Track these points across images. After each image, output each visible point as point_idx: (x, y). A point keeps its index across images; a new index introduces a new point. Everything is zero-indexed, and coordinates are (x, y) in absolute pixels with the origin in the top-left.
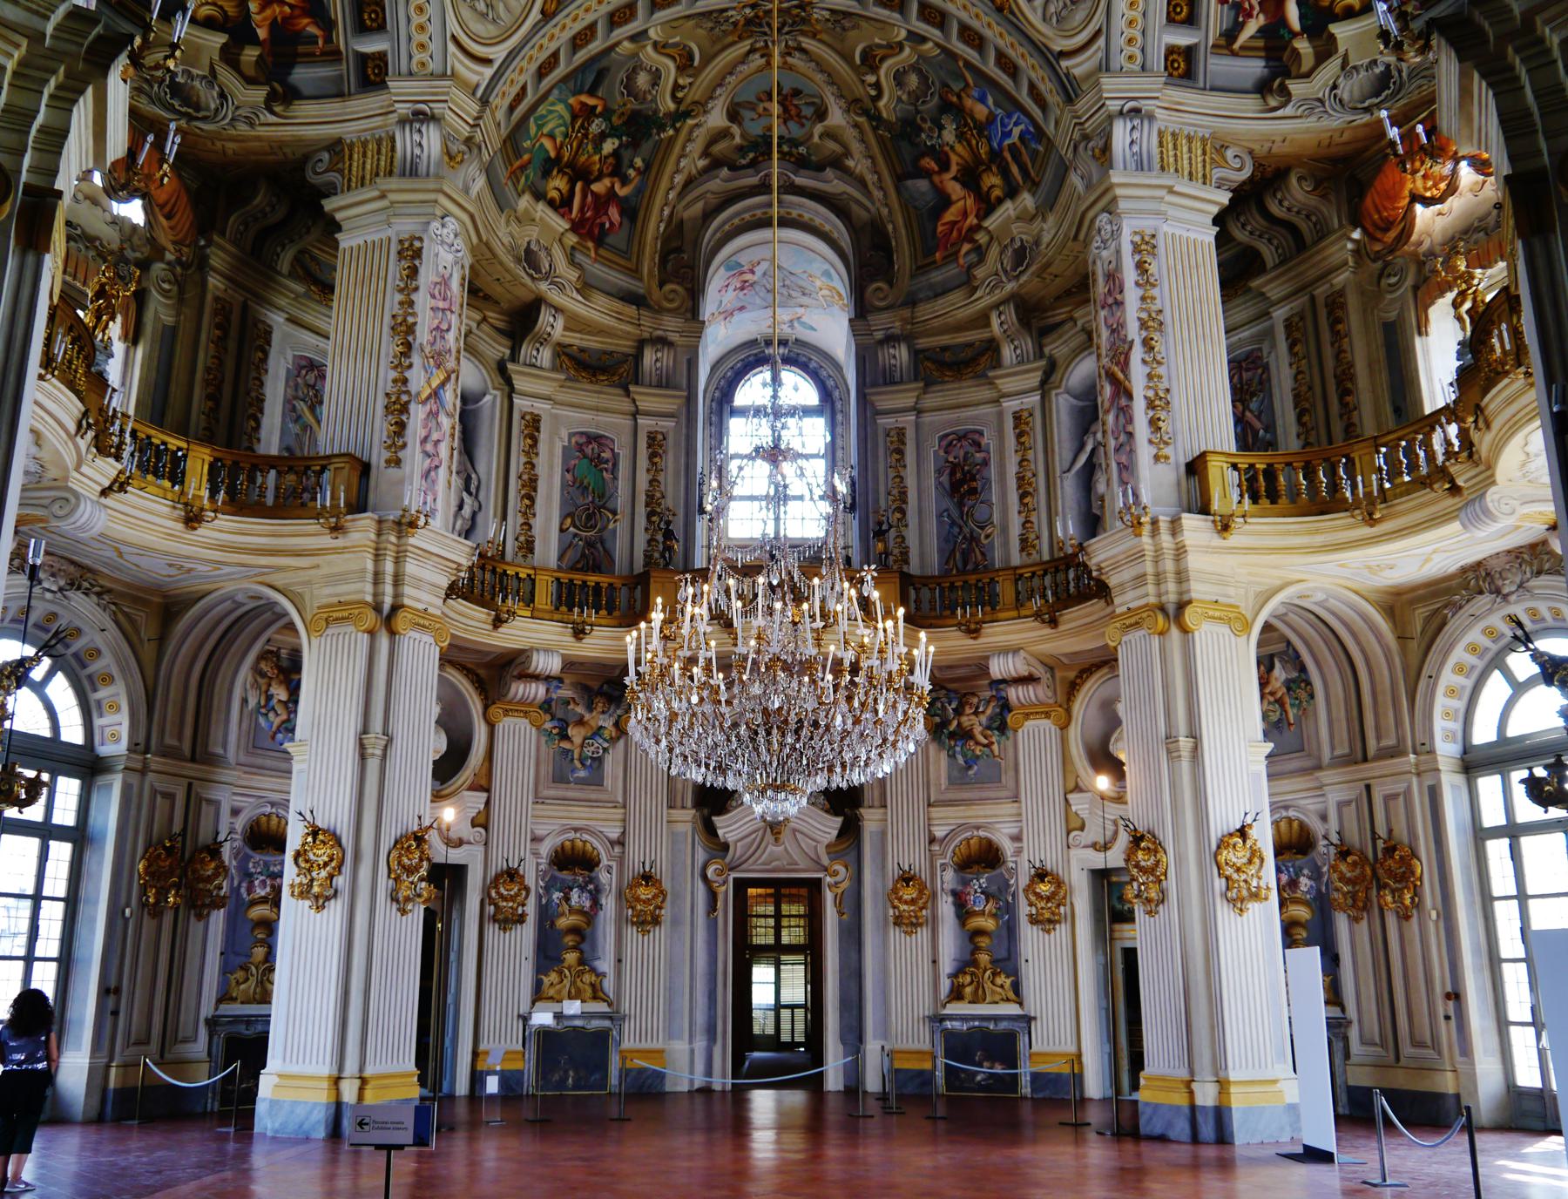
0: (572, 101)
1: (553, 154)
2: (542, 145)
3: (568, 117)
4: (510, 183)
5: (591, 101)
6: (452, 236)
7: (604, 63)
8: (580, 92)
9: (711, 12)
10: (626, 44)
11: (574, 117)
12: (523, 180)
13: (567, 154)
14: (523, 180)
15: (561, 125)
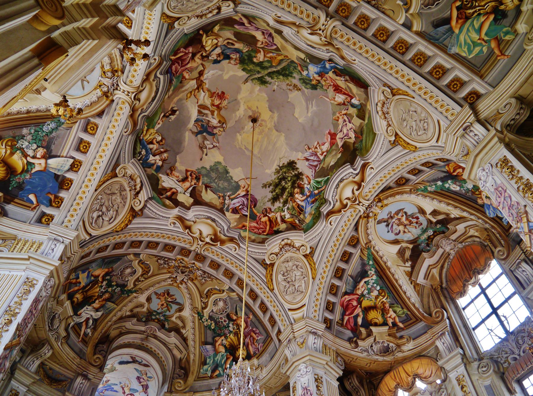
0: (457, 31)
1: (492, 17)
2: (486, 34)
3: (470, 21)
4: (507, 54)
5: (455, 13)
6: (484, 173)
7: (431, 30)
8: (451, 30)
9: (373, 6)
10: (415, 28)
11: (467, 18)
12: (507, 38)
13: (491, 4)
14: (507, 38)
15: (473, 25)
